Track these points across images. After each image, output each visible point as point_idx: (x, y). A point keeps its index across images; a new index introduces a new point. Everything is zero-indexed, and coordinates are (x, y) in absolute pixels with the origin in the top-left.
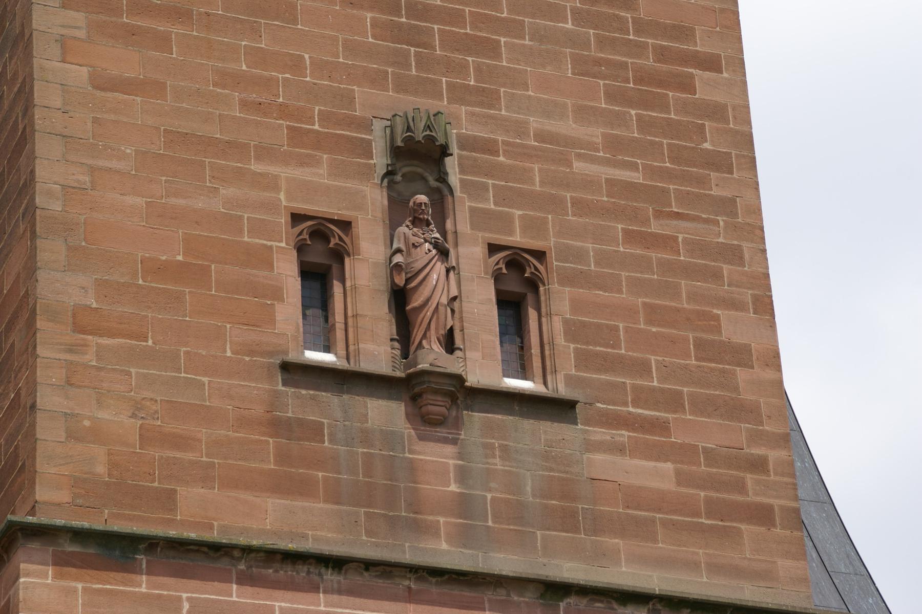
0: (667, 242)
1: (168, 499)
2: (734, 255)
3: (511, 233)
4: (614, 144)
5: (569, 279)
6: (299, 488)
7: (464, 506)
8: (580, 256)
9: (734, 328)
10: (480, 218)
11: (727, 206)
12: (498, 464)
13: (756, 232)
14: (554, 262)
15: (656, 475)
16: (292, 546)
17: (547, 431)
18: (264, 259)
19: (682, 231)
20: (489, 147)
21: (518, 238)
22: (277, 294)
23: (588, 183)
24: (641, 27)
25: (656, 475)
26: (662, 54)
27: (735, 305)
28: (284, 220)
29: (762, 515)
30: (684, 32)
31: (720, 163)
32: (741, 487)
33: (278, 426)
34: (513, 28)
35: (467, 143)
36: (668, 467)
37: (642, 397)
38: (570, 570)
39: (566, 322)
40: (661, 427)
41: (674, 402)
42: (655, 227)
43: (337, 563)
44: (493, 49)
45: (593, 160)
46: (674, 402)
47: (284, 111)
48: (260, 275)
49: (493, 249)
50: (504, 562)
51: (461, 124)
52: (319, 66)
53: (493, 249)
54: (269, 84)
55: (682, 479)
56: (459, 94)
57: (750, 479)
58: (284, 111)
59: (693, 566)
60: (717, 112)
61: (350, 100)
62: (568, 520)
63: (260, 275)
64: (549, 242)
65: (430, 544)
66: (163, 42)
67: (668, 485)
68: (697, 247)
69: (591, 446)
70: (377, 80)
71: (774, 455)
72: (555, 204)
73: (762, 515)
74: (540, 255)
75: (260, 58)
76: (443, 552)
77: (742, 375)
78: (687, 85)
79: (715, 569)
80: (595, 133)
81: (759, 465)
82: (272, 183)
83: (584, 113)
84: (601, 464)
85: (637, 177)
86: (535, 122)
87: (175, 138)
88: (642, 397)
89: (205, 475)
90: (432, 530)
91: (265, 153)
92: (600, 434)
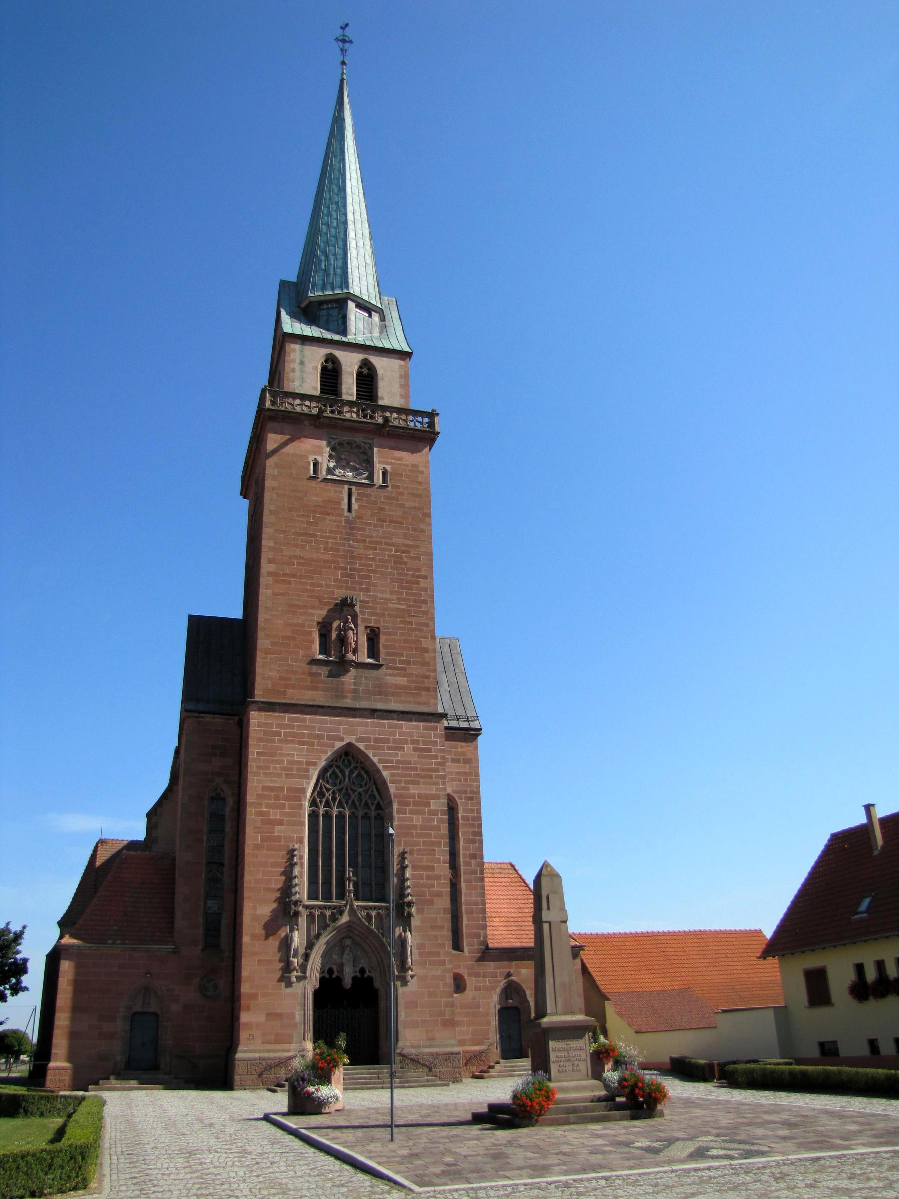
0: (410, 623)
1: (284, 693)
2: (427, 625)
4: (399, 599)
6: (316, 689)
7: (355, 691)
9: (425, 644)
10: (363, 621)
11: (426, 613)
12: (363, 680)
13: (432, 619)
14: (381, 630)
15: (401, 681)
16: (311, 703)
17: (374, 673)
18: (310, 633)
19: (414, 620)
20: (367, 602)
21: (372, 625)
22: (313, 642)
24: (408, 569)
25: (401, 681)
26: (413, 576)
27: (425, 638)
28: (315, 624)
29: (427, 689)
30: (418, 570)
31: (425, 602)
32: (423, 682)
33: (311, 674)
34: (375, 572)
35: (361, 602)
36: (405, 679)
37: (401, 662)
38: (379, 706)
40: (404, 669)
41: (408, 663)
42: (407, 620)
43: (322, 707)
44: (370, 577)
46: (408, 663)
47: (318, 597)
49: (366, 628)
50: (364, 704)
51: (359, 596)
52: (327, 585)
53: (366, 628)
54: (314, 591)
55: (408, 682)
56: (361, 590)
57: (425, 681)
58: (318, 597)
59: (409, 702)
60: (425, 589)
61: (333, 592)
62: (380, 694)
64: (381, 625)
65: (345, 701)
66: (289, 583)
67: (405, 683)
68: (417, 624)
69: (386, 675)
70: (340, 587)
71: (432, 674)
72: (383, 615)
73: (427, 689)
74: (378, 628)
75: (312, 584)
76: (348, 703)
77: (426, 655)
78: (418, 583)
79: (415, 703)
80: (394, 597)
81: (428, 677)
82: (313, 615)
83: (392, 592)
84: (389, 679)
85: (404, 607)
86: (379, 595)
87: (291, 606)
88: (401, 662)
89: (293, 687)
90: (346, 697)
91: (312, 608)
92: (389, 672)
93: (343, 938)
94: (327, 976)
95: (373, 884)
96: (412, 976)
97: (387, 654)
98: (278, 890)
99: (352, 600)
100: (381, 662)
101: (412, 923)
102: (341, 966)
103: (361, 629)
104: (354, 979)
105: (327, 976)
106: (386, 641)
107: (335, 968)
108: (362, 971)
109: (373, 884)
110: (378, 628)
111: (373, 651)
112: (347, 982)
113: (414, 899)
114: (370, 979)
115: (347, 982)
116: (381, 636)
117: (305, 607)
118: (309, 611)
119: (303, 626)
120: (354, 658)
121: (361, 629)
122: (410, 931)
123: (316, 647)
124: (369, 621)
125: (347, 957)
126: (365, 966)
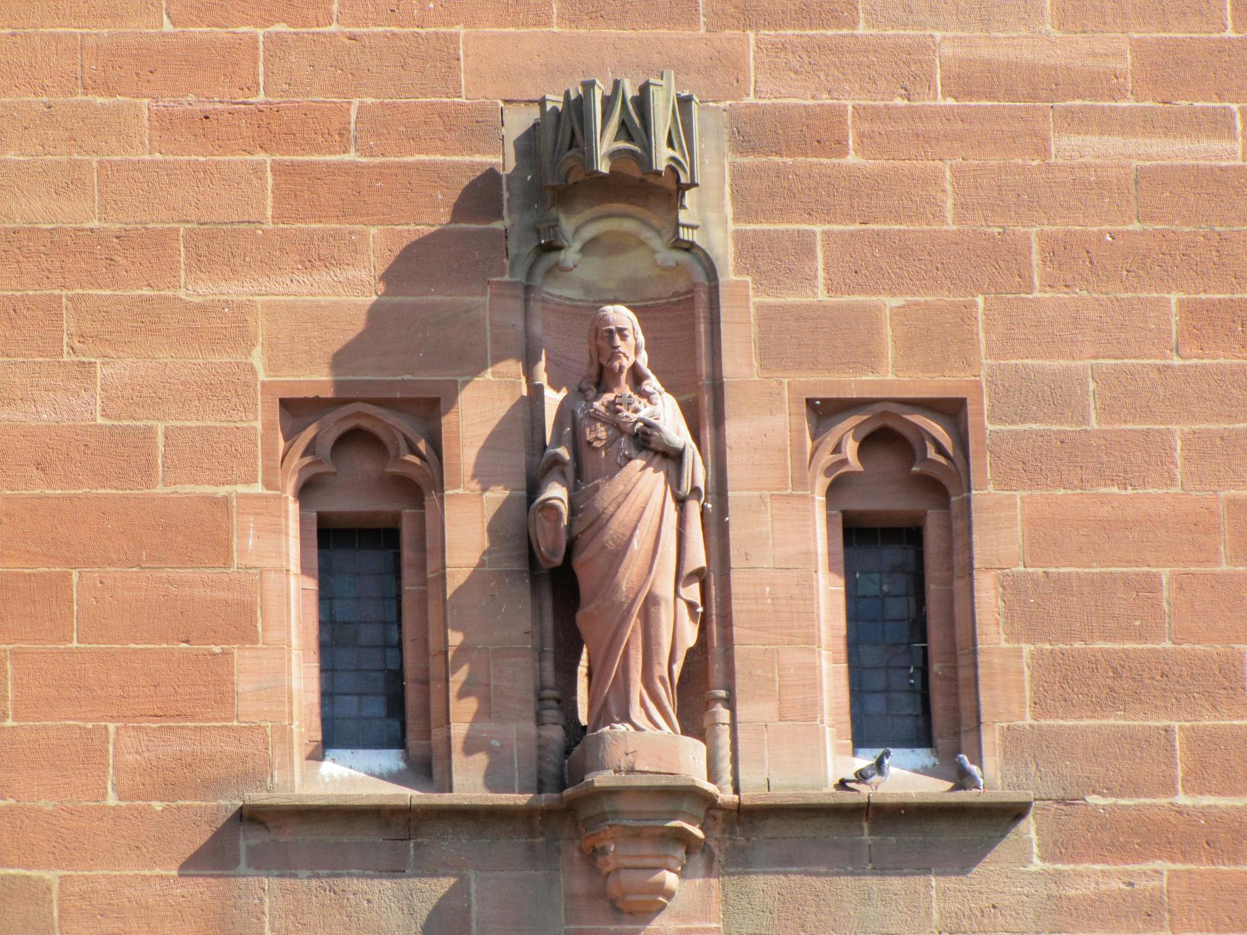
3: (871, 359)
4: (1167, 69)
5: (1033, 465)
8: (1059, 397)
10: (784, 338)
14: (987, 425)
18: (208, 533)
20: (821, 133)
21: (889, 375)
22: (241, 622)
23: (1089, 188)
28: (260, 420)
35: (750, 134)
39: (1011, 586)
45: (1108, 123)
47: (269, 128)
48: (196, 581)
49: (823, 412)
53: (823, 412)
54: (228, 60)
58: (269, 128)
63: (196, 581)
64: (971, 374)
72: (999, 262)
74: (952, 411)
82: (232, 327)
86: (950, 42)
91: (217, 248)
97: (1062, 683)
99: (636, 125)
100: (993, 779)
103: (763, 426)
106: (1044, 536)
110: (952, 411)
111: (908, 662)
116: (986, 494)
117: (148, 249)
118: (195, 290)
119: (126, 453)
120: (689, 761)
121: (763, 426)
123: (286, 666)
124: (850, 334)
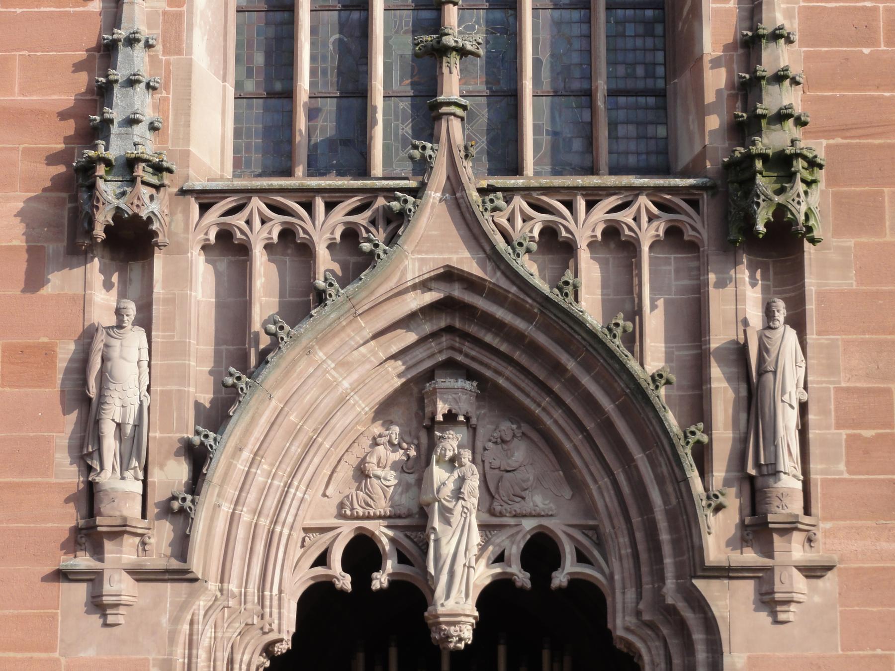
93: (429, 375)
94: (345, 582)
95: (601, 86)
96: (813, 572)
98: (63, 116)
101: (812, 283)
102: (415, 525)
104: (493, 599)
105: (345, 582)
107: (382, 533)
108: (541, 552)
109: (601, 86)
112: (457, 609)
113: (819, 148)
114: (588, 598)
115: (457, 609)
122: (798, 322)
125: (457, 481)
126: (556, 526)
